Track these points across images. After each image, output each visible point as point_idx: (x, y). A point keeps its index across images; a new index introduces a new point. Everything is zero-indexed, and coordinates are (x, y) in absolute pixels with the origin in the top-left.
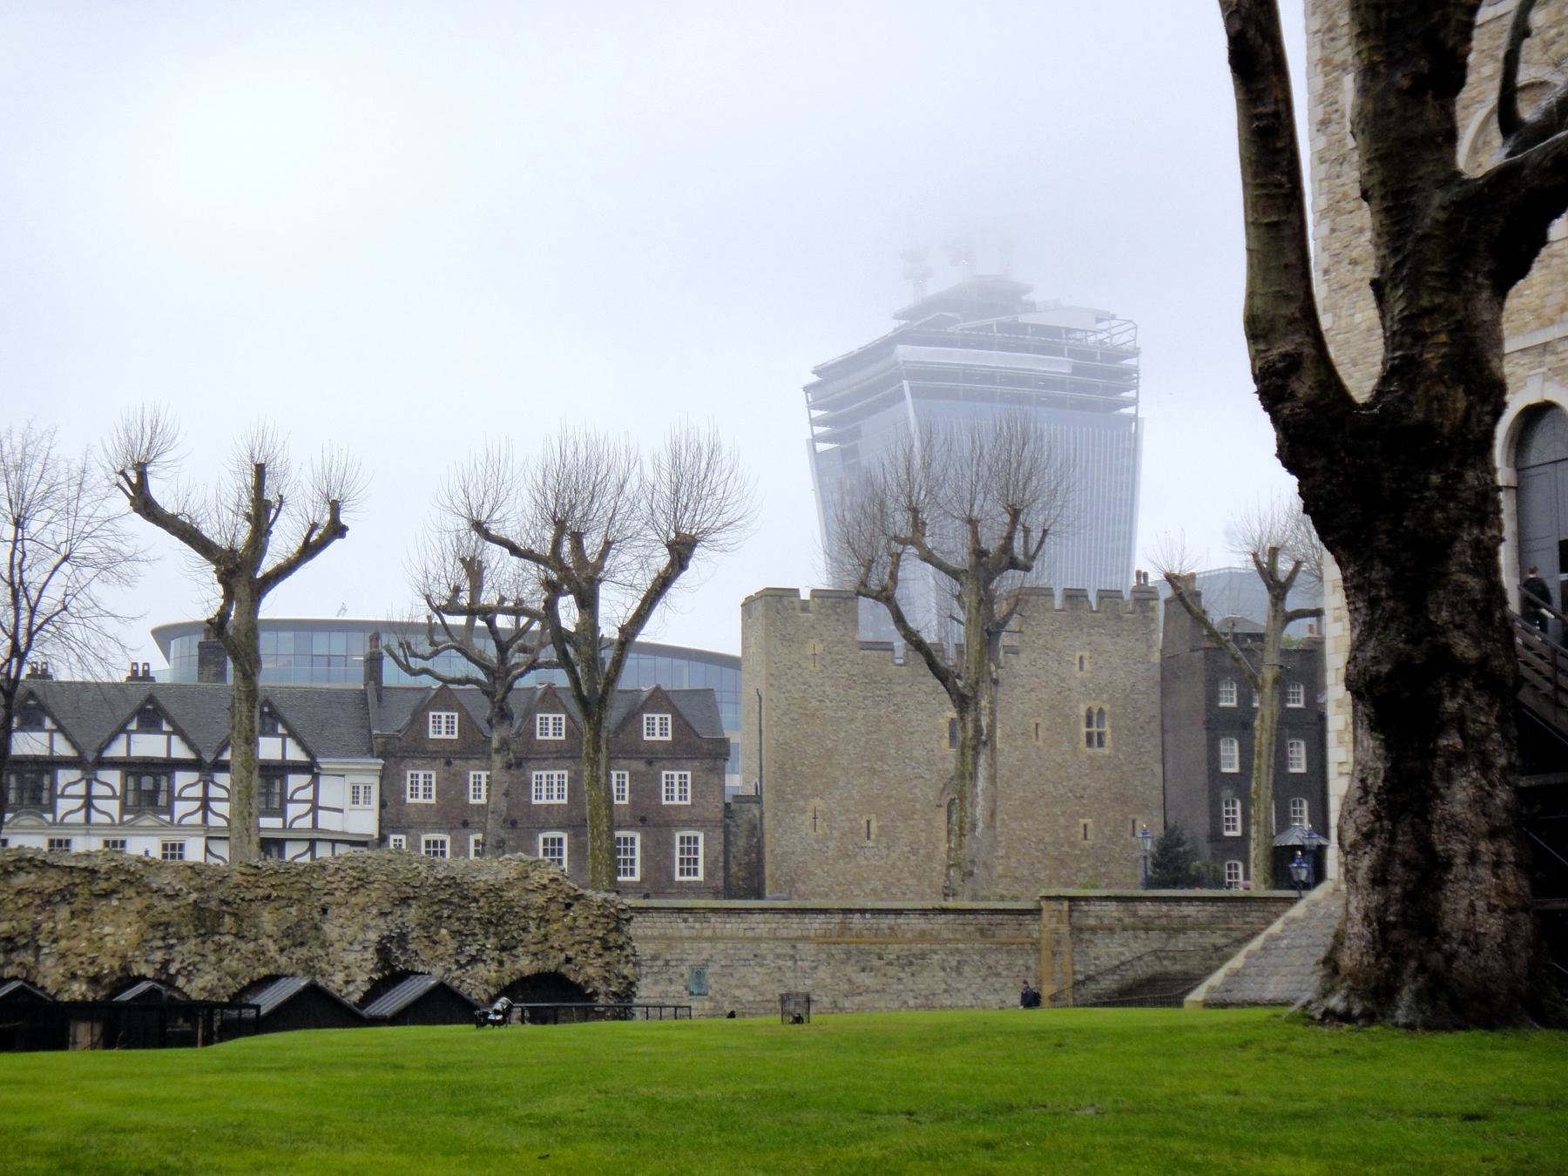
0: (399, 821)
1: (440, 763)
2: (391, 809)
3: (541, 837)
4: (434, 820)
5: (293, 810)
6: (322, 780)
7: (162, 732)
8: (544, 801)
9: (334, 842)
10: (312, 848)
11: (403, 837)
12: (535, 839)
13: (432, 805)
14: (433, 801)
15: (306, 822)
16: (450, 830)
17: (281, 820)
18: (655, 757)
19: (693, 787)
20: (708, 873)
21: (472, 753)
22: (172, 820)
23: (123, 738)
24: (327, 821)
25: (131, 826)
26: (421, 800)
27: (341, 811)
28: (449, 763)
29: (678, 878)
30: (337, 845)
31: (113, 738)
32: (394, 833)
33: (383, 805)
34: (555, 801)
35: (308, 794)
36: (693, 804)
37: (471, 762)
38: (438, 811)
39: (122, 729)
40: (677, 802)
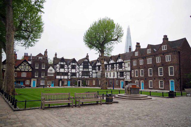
5: (123, 68)
8: (149, 63)
9: (128, 72)
10: (126, 73)
15: (124, 69)
16: (138, 69)
18: (164, 53)
19: (171, 58)
20: (175, 74)
24: (126, 69)
29: (169, 75)
33: (131, 66)
34: (150, 63)
35: (124, 66)
36: (171, 61)
39: (110, 60)
40: (168, 61)
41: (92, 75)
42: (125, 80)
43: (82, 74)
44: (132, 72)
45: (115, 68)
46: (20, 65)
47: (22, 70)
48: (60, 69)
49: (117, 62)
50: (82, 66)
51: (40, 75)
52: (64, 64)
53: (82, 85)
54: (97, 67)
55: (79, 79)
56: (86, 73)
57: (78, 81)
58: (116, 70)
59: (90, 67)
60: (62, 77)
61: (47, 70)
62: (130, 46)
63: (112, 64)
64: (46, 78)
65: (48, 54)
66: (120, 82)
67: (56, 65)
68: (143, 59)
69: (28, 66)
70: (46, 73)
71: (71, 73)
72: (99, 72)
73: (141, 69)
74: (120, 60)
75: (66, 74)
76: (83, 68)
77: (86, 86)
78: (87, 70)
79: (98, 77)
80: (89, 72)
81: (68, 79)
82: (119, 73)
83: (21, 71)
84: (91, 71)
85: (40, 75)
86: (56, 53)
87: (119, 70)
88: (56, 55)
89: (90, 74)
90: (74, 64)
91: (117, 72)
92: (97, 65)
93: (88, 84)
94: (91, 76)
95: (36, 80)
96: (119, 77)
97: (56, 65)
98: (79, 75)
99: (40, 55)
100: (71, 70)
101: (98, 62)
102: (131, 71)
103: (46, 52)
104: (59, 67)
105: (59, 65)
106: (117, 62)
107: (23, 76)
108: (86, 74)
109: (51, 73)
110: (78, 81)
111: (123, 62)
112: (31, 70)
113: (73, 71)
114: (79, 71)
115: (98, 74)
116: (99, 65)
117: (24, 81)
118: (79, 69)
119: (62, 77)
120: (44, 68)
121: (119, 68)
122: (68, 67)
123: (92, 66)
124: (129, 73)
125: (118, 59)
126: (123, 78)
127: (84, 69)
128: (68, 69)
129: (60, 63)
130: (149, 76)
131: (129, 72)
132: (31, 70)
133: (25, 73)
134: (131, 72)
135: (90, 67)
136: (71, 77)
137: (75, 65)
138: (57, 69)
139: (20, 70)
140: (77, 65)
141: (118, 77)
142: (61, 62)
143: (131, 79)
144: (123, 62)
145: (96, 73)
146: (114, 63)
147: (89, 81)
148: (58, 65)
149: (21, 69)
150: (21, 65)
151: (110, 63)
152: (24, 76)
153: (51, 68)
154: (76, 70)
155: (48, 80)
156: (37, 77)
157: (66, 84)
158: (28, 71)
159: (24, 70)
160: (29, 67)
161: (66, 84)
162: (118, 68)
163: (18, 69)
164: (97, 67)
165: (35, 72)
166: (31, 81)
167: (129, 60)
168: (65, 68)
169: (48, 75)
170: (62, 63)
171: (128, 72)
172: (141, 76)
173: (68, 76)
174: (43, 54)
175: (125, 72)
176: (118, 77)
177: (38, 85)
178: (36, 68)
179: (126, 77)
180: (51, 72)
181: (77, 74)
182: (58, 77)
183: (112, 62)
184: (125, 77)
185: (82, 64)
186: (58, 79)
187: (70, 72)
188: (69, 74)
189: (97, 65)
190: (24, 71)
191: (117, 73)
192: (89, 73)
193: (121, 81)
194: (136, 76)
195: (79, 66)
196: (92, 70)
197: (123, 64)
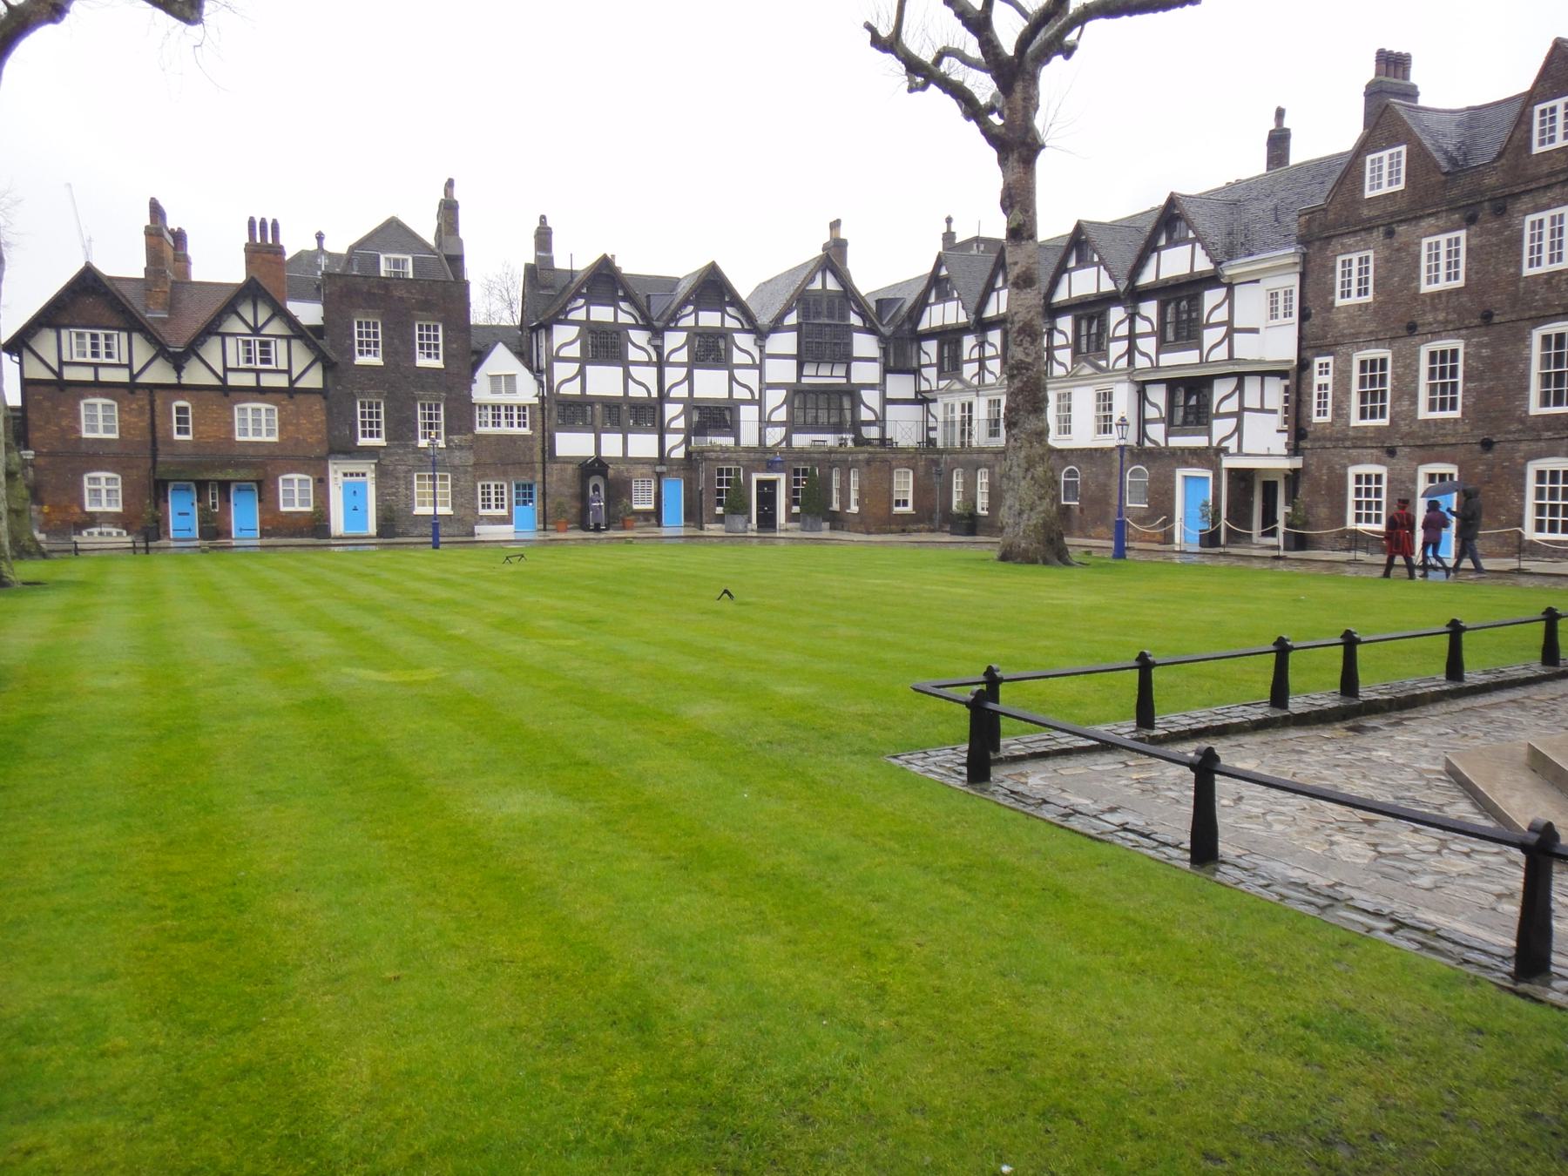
0: (1325, 337)
1: (1378, 234)
2: (1315, 320)
3: (1537, 335)
4: (1371, 327)
6: (1239, 292)
7: (1093, 264)
9: (1263, 374)
10: (1240, 387)
11: (1330, 359)
12: (1524, 339)
13: (1367, 305)
14: (1369, 298)
15: (1221, 354)
17: (1198, 351)
21: (1425, 207)
22: (1108, 365)
23: (1066, 276)
24: (1246, 348)
25: (1075, 375)
26: (1354, 299)
27: (1255, 331)
28: (1390, 234)
30: (1268, 380)
31: (1054, 284)
32: (1318, 355)
33: (1304, 316)
35: (1221, 315)
37: (1424, 224)
38: (1376, 312)
41: (880, 421)
42: (1228, 463)
43: (790, 413)
44: (1318, 379)
45: (1117, 349)
46: (212, 329)
47: (234, 380)
48: (590, 369)
49: (1147, 277)
50: (785, 342)
51: (401, 429)
52: (624, 319)
53: (791, 517)
54: (931, 347)
55: (764, 457)
56: (822, 404)
57: (755, 477)
58: (1131, 362)
59: (865, 345)
60: (612, 445)
61: (471, 379)
62: (1280, 114)
63: (1091, 310)
64: (458, 457)
65: (464, 231)
66: (1173, 482)
67: (547, 327)
68: (1470, 221)
69: (288, 338)
70: (462, 414)
71: (691, 404)
72: (948, 391)
73: (1436, 335)
74: (1174, 262)
75: (646, 414)
76: (801, 361)
77: (832, 528)
78: (840, 371)
79: (938, 435)
80: (852, 393)
81: (662, 458)
82: (1158, 395)
83: (225, 391)
84: (871, 387)
85: (401, 429)
86: (543, 218)
87: (1167, 359)
88: (543, 237)
89: (865, 415)
90: (710, 319)
91: (1141, 390)
92: (924, 325)
93: (845, 503)
94: (873, 433)
95: (368, 468)
96: (1157, 432)
97: (549, 330)
98: (764, 423)
99: (393, 233)
100: (689, 377)
101: (944, 297)
102: (1303, 365)
103: (449, 210)
104: (575, 351)
105: (575, 330)
106: (1147, 277)
107: (251, 438)
108: (823, 417)
109: (509, 408)
110: (755, 477)
111: (1212, 280)
112: (314, 379)
113: (711, 384)
114: (766, 386)
115: (937, 409)
116: (950, 320)
117: (259, 483)
118: (760, 367)
119: (612, 445)
120: (438, 363)
121: (1163, 346)
122: (659, 350)
123: (883, 339)
124: (1275, 393)
125: (1150, 248)
126: (1200, 441)
127: (809, 370)
128: (661, 364)
129: (580, 315)
130: (1535, 408)
131: (1282, 374)
132: (314, 379)
133: (263, 406)
134: (1296, 376)
135: (865, 345)
136: (687, 441)
137: (723, 334)
138: (562, 371)
139: (215, 382)
140: (743, 330)
141: (1142, 434)
142: (588, 304)
143: (1294, 450)
144: (1212, 280)
145: (922, 400)
146: (1104, 301)
147: (854, 478)
148: (563, 335)
149: (226, 369)
150: (224, 335)
151: (1061, 295)
152: (257, 432)
153: (501, 360)
154: (737, 373)
155: (481, 469)
156: (380, 441)
157: (651, 507)
158: (291, 391)
159: (248, 380)
160: (296, 344)
161: (651, 507)
162: (1148, 345)
163: (196, 375)
164: (931, 347)
165: (352, 398)
166: (322, 483)
167: (1289, 254)
168: (634, 354)
169: (479, 430)
170: (603, 314)
171: (1263, 374)
172: (1423, 413)
173: (662, 430)
174: (426, 228)
175: (1233, 382)
176: (1142, 434)
177: (392, 524)
178: (360, 360)
179: (1239, 429)
180: (503, 398)
181: (748, 415)
182: (573, 444)
183: (1084, 282)
184: (1221, 428)
185: (792, 319)
186: (568, 460)
187: (681, 392)
188: (671, 410)
189: (924, 325)
190: (259, 392)
191: (1142, 397)
192: (857, 402)
193: (1180, 473)
194: (1355, 421)
195: (761, 334)
196: (887, 370)
197: (1212, 297)
